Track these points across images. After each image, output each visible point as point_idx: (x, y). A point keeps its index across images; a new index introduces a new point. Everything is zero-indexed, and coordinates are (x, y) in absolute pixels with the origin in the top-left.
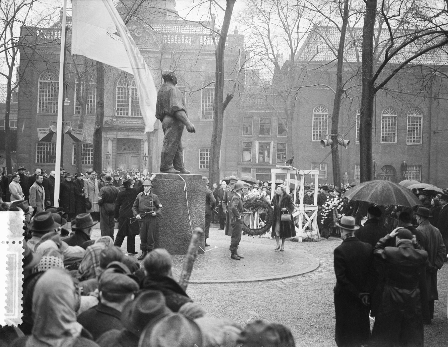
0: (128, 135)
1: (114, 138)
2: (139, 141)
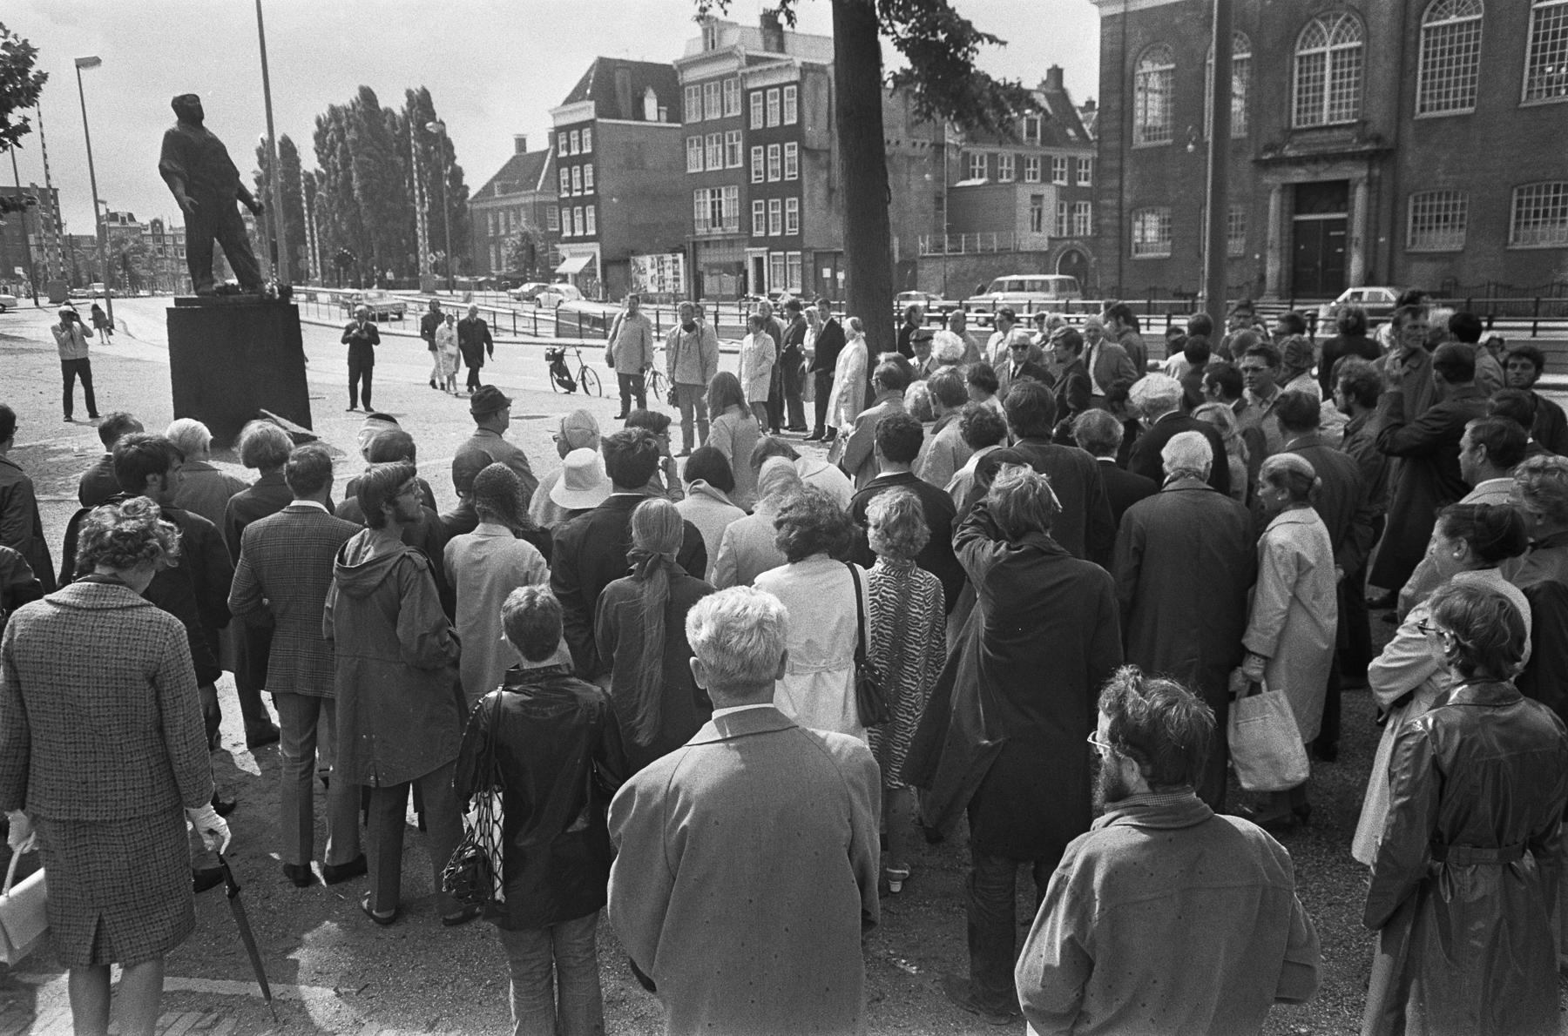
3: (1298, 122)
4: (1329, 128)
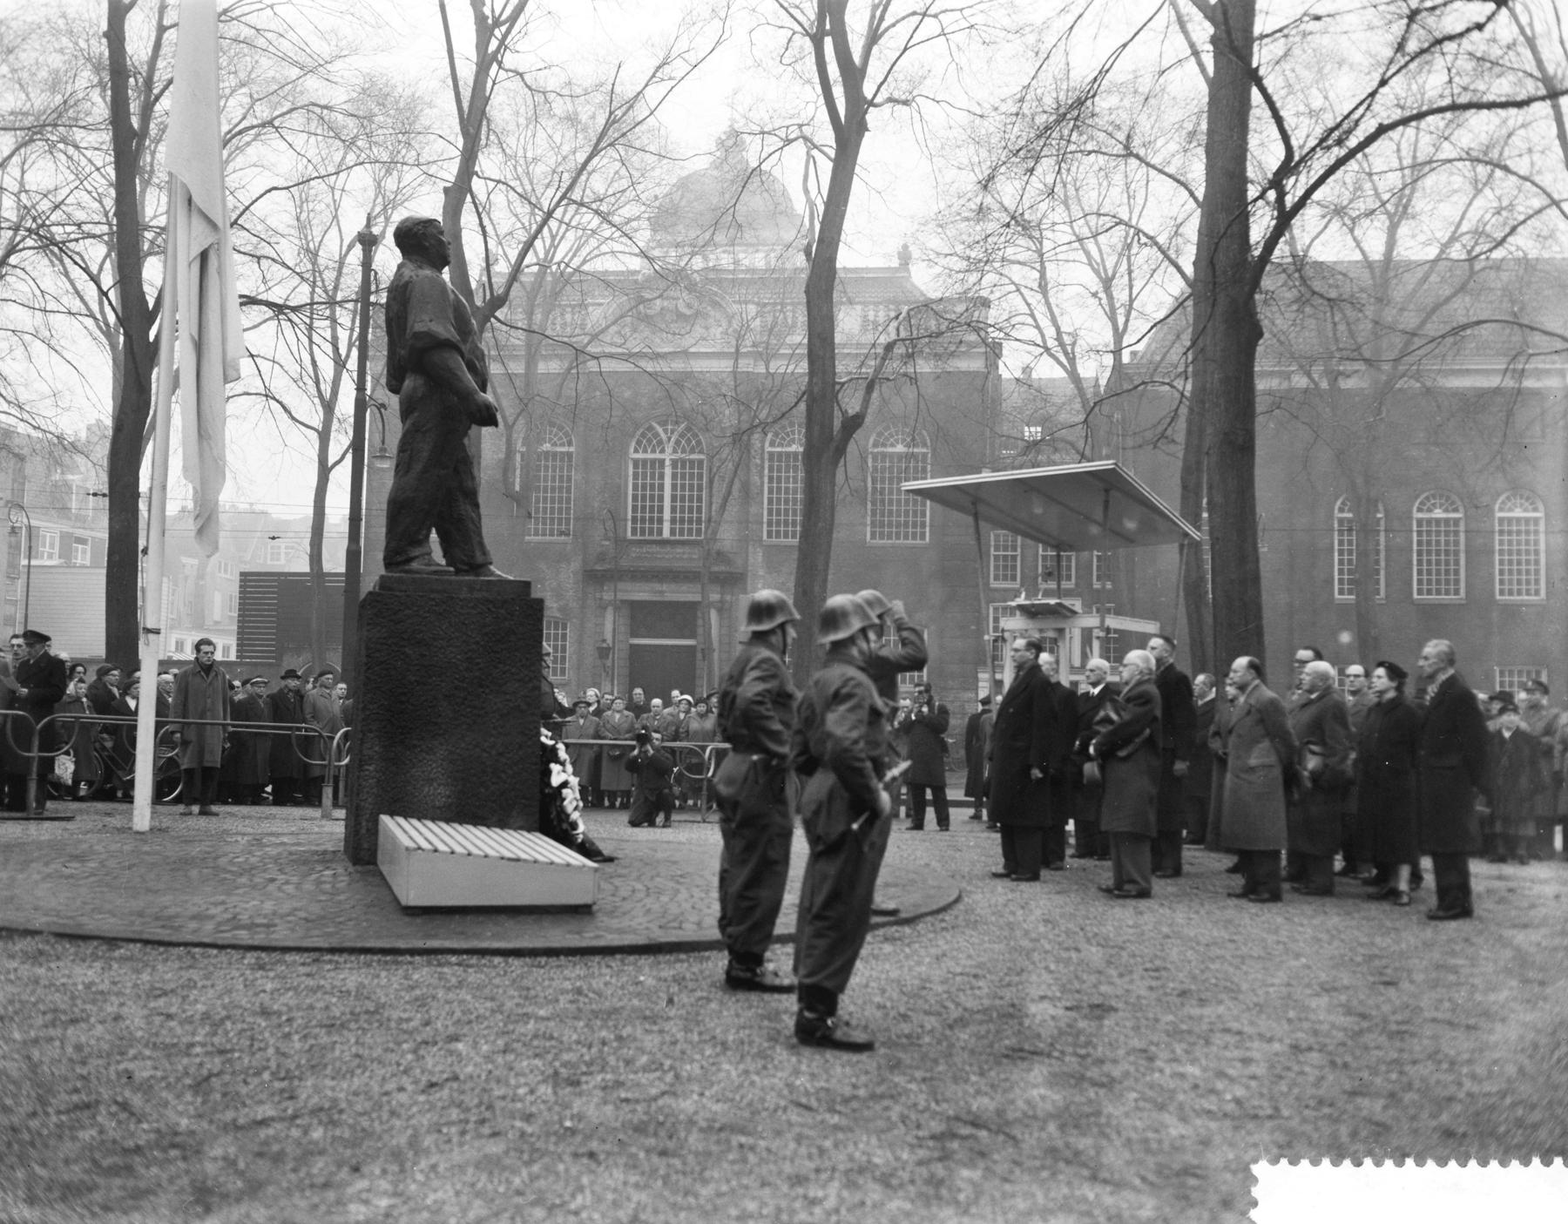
0: (662, 592)
1: (623, 602)
2: (692, 607)
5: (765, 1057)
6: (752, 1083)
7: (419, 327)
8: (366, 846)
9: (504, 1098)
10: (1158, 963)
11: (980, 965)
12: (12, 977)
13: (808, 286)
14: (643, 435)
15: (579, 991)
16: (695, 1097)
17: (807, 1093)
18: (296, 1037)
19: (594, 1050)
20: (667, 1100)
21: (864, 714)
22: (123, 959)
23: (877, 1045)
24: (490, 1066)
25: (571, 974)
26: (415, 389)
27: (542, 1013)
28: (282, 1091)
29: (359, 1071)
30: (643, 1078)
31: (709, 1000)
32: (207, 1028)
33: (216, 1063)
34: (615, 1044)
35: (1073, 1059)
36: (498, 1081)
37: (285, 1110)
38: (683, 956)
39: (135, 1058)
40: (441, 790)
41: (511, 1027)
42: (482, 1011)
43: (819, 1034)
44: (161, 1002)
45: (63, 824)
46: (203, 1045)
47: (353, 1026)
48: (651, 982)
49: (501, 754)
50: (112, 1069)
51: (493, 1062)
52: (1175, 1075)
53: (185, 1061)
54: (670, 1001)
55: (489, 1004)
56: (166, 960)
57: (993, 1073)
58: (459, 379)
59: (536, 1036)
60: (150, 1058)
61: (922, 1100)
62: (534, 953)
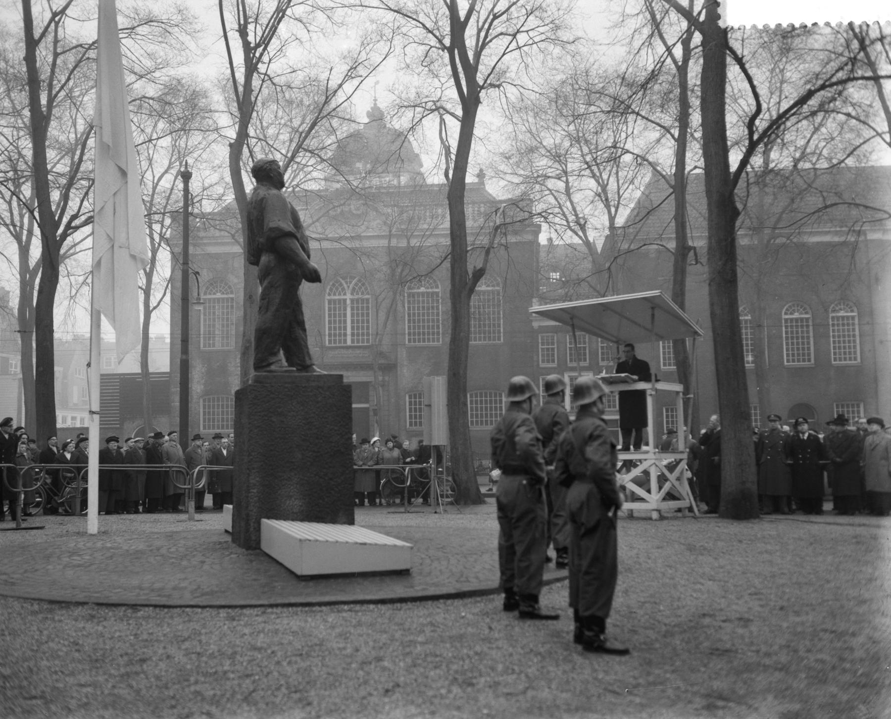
3: (330, 342)
4: (350, 347)
5: (570, 661)
6: (573, 678)
7: (272, 225)
8: (254, 538)
9: (435, 696)
10: (753, 589)
11: (652, 596)
12: (85, 633)
13: (449, 194)
14: (334, 285)
15: (431, 624)
16: (547, 690)
17: (610, 684)
18: (285, 664)
19: (467, 662)
20: (530, 693)
21: (608, 447)
22: (147, 618)
23: (631, 650)
24: (413, 677)
25: (418, 615)
26: (269, 261)
27: (420, 639)
28: (300, 700)
29: (337, 684)
30: (511, 678)
31: (513, 627)
32: (228, 662)
33: (247, 684)
34: (477, 658)
35: (753, 654)
36: (426, 686)
37: (310, 713)
38: (479, 599)
39: (196, 682)
40: (297, 502)
41: (408, 650)
42: (384, 641)
43: (596, 645)
44: (187, 645)
45: (40, 531)
46: (233, 672)
47: (313, 653)
48: (470, 616)
49: (331, 479)
50: (187, 690)
51: (413, 673)
52: (817, 661)
53: (228, 683)
54: (490, 628)
55: (385, 636)
56: (172, 617)
57: (711, 665)
58: (297, 255)
59: (426, 655)
60: (205, 683)
61: (680, 683)
62: (392, 601)
